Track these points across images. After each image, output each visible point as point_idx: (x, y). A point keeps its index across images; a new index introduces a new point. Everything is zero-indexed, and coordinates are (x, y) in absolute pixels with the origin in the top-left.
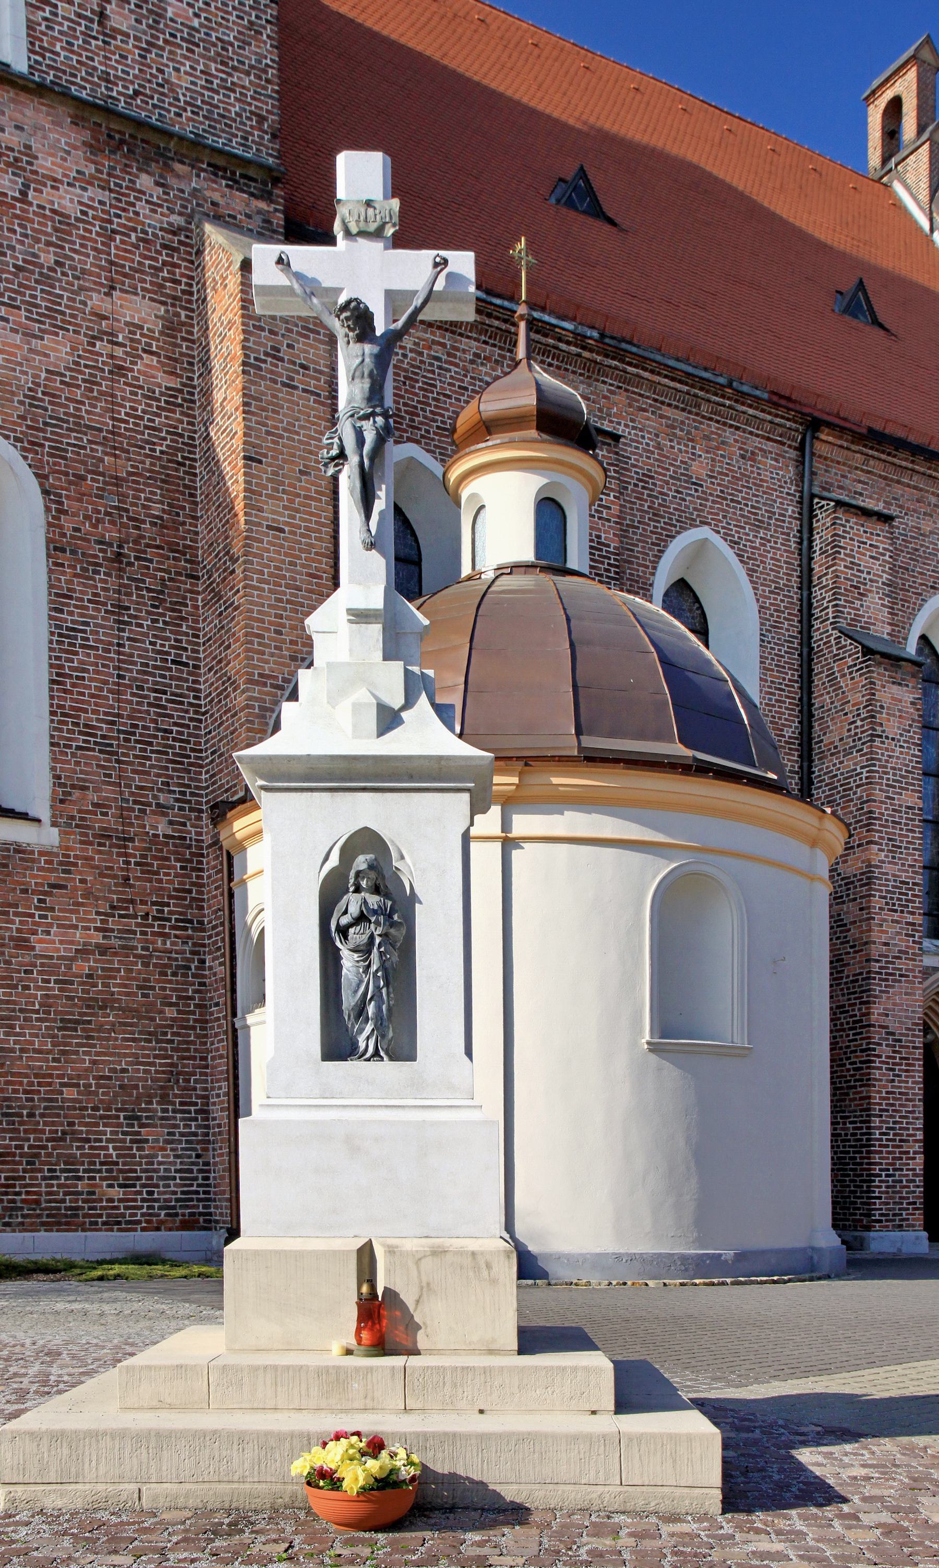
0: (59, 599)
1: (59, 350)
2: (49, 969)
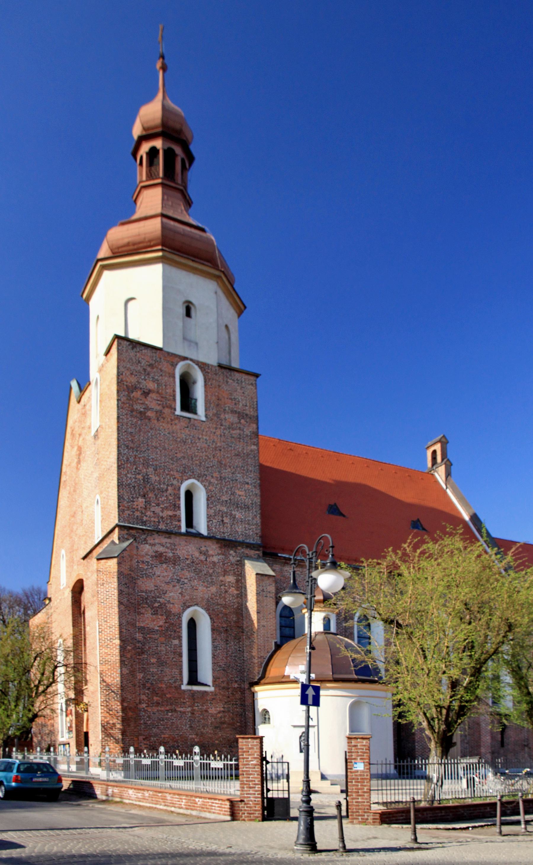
0: (214, 640)
1: (213, 589)
2: (212, 716)
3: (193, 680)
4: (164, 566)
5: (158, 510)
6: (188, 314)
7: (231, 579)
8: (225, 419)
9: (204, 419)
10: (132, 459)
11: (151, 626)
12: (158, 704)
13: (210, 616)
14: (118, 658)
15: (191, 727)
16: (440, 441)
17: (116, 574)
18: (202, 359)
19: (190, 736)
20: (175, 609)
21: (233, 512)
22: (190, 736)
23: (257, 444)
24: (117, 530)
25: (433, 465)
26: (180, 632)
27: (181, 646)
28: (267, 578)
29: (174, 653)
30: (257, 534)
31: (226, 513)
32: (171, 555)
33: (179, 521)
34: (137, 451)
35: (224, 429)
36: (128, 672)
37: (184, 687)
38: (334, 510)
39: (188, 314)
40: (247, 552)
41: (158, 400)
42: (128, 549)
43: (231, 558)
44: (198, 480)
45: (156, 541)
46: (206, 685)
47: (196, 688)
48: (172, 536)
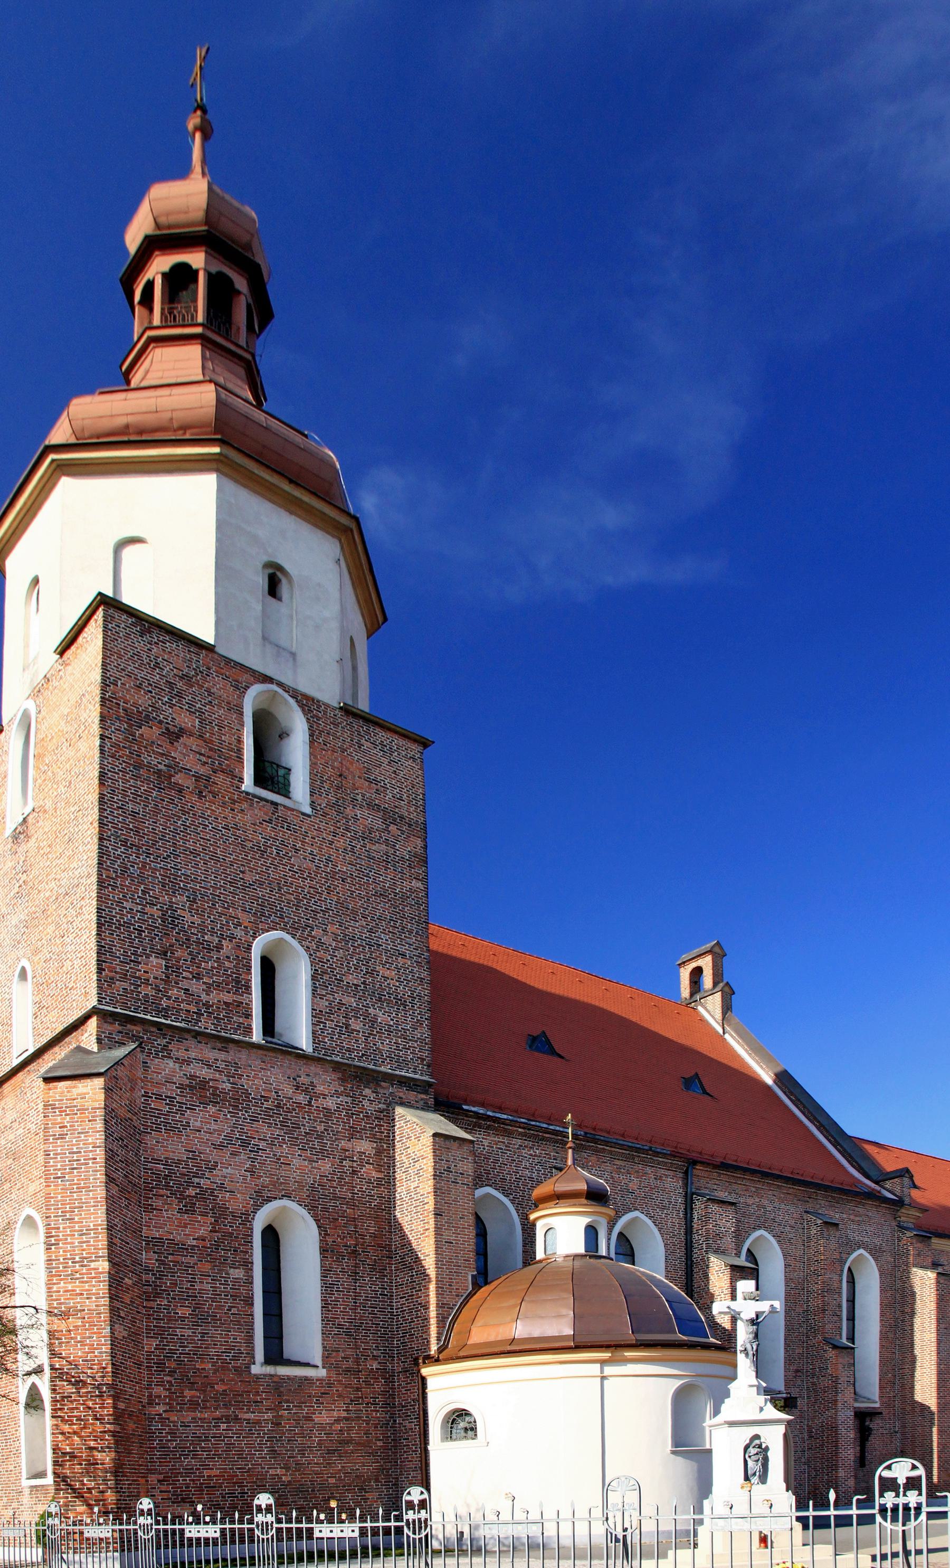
0: (325, 1272)
1: (326, 1166)
2: (322, 1428)
3: (275, 1355)
4: (212, 1109)
5: (196, 987)
6: (273, 588)
7: (365, 1146)
8: (356, 819)
9: (308, 810)
10: (135, 871)
11: (179, 1236)
12: (194, 1405)
13: (317, 1221)
14: (105, 1301)
15: (273, 1451)
16: (710, 952)
17: (100, 1113)
18: (304, 686)
19: (271, 1472)
20: (237, 1202)
21: (371, 1010)
22: (271, 1472)
23: (425, 880)
24: (93, 1022)
25: (692, 995)
26: (248, 1252)
27: (251, 1282)
28: (456, 1144)
29: (234, 1297)
30: (423, 1060)
31: (356, 1010)
32: (228, 1086)
33: (248, 1016)
34: (149, 855)
35: (353, 838)
36: (125, 1334)
37: (256, 1369)
38: (540, 1043)
39: (273, 588)
40: (401, 1095)
41: (201, 754)
42: (125, 1062)
43: (366, 1103)
44: (294, 936)
45: (193, 1055)
46: (307, 1365)
47: (283, 1371)
48: (231, 1045)
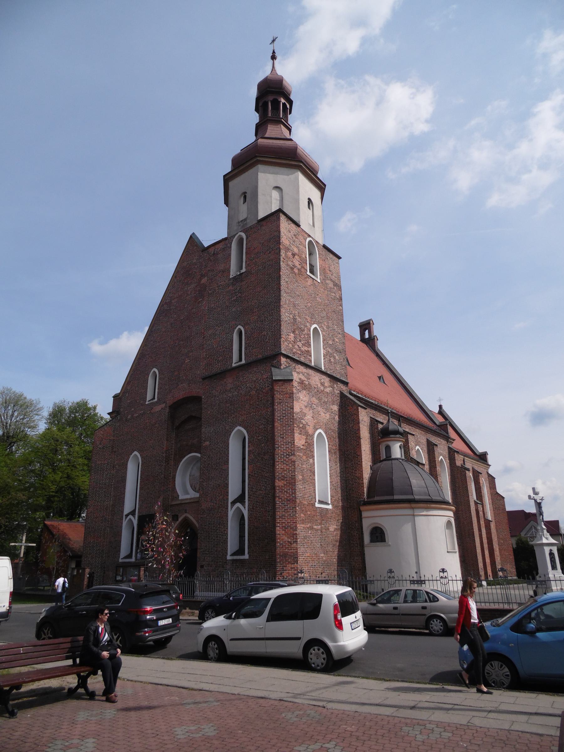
32: (307, 383)
33: (311, 356)
